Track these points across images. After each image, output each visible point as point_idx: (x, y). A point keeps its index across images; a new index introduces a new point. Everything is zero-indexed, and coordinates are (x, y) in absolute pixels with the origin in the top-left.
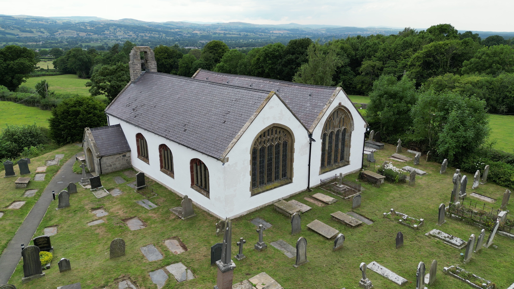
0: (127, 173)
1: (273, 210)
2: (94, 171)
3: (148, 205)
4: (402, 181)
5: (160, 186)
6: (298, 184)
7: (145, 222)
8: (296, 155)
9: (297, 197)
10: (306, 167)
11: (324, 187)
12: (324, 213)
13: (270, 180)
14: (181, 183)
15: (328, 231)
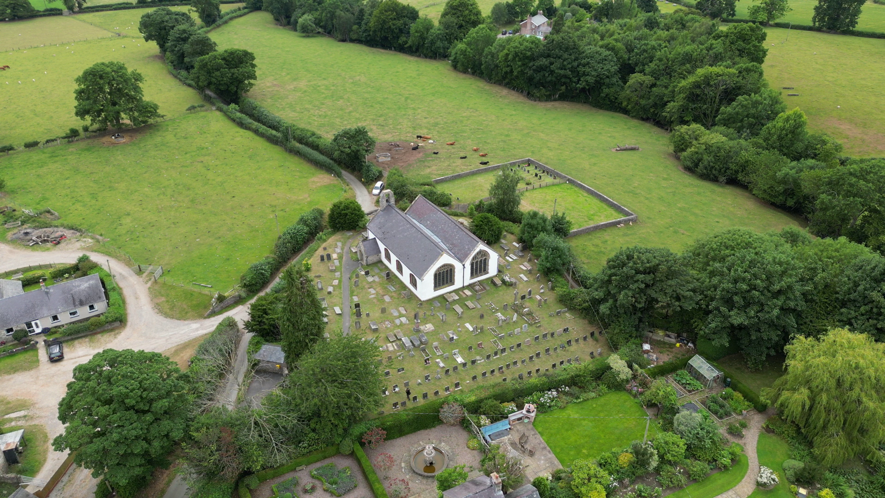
0: (379, 265)
1: (442, 297)
2: (362, 260)
3: (392, 289)
4: (511, 285)
5: (397, 277)
6: (458, 284)
7: (391, 297)
8: (456, 274)
9: (455, 291)
10: (463, 276)
11: (471, 287)
12: (461, 301)
13: (443, 284)
14: (405, 278)
15: (459, 309)
